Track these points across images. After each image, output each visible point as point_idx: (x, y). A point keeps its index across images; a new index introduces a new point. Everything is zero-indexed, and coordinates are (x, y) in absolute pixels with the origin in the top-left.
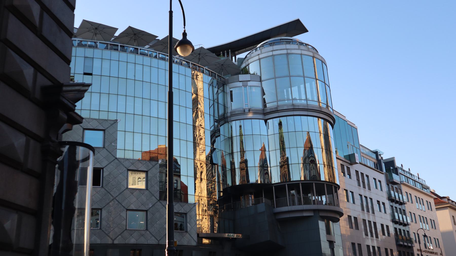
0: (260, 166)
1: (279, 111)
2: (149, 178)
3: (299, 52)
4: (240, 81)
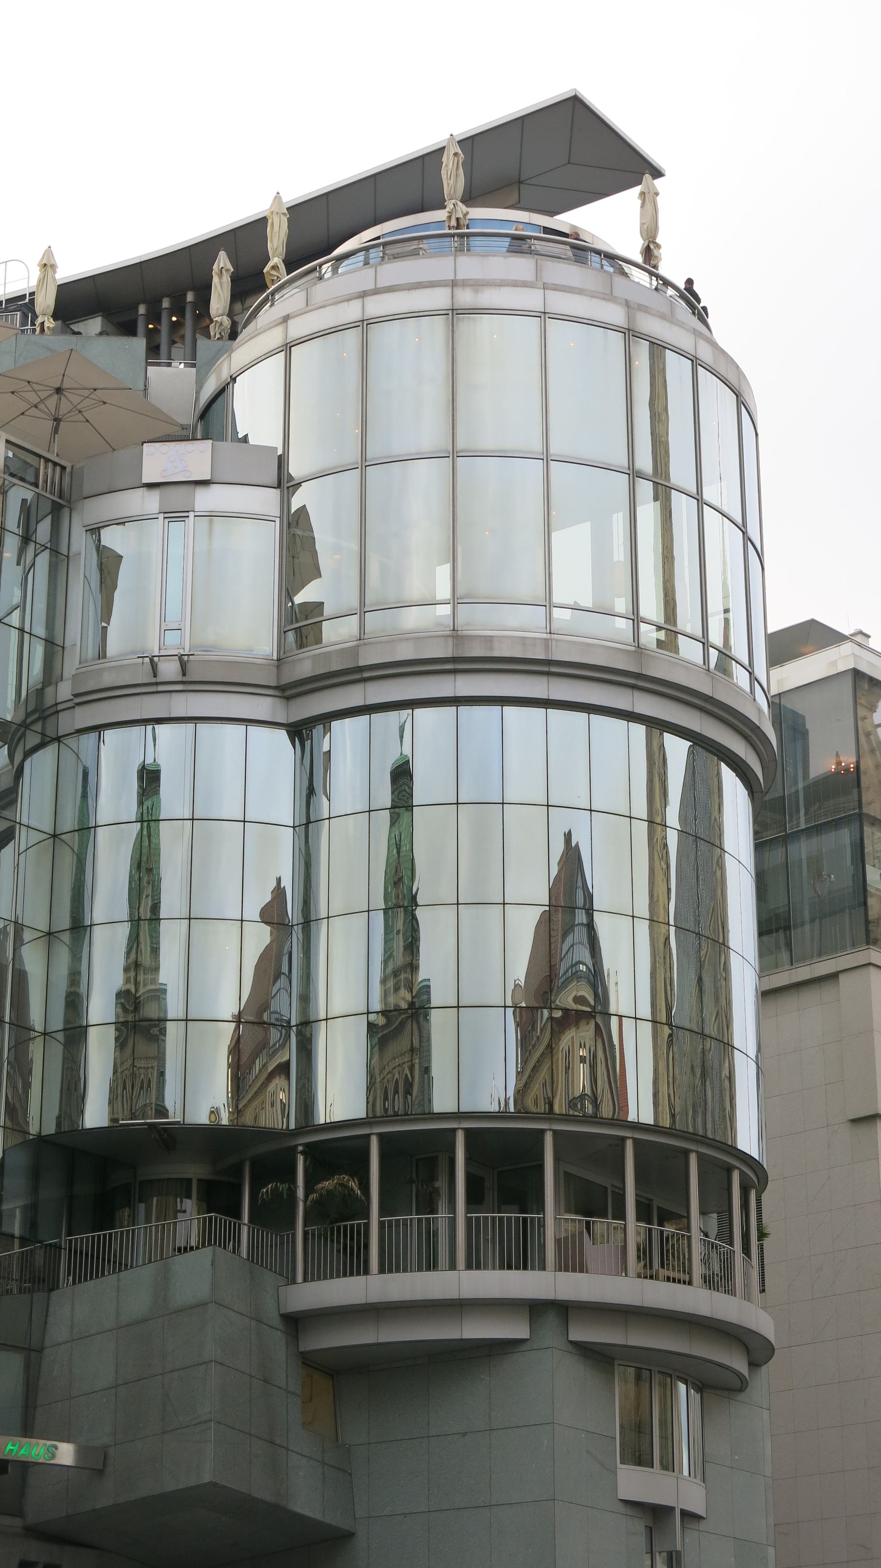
0: (238, 1019)
1: (366, 675)
3: (532, 299)
4: (145, 480)
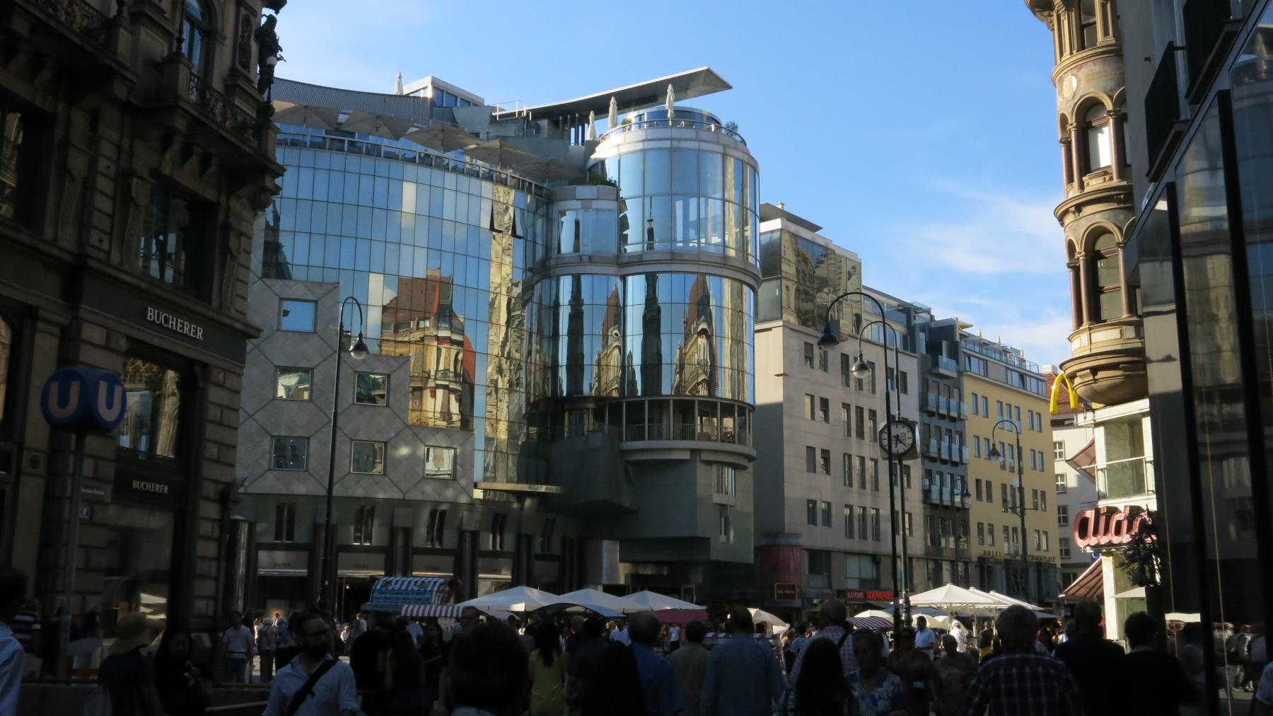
2: (392, 387)
